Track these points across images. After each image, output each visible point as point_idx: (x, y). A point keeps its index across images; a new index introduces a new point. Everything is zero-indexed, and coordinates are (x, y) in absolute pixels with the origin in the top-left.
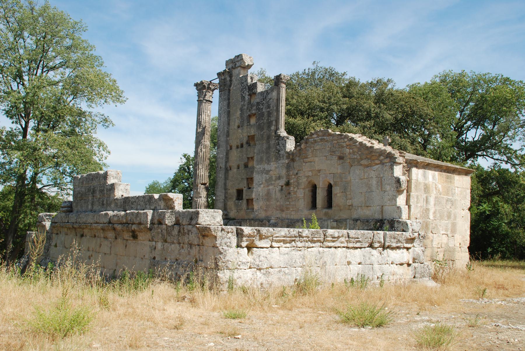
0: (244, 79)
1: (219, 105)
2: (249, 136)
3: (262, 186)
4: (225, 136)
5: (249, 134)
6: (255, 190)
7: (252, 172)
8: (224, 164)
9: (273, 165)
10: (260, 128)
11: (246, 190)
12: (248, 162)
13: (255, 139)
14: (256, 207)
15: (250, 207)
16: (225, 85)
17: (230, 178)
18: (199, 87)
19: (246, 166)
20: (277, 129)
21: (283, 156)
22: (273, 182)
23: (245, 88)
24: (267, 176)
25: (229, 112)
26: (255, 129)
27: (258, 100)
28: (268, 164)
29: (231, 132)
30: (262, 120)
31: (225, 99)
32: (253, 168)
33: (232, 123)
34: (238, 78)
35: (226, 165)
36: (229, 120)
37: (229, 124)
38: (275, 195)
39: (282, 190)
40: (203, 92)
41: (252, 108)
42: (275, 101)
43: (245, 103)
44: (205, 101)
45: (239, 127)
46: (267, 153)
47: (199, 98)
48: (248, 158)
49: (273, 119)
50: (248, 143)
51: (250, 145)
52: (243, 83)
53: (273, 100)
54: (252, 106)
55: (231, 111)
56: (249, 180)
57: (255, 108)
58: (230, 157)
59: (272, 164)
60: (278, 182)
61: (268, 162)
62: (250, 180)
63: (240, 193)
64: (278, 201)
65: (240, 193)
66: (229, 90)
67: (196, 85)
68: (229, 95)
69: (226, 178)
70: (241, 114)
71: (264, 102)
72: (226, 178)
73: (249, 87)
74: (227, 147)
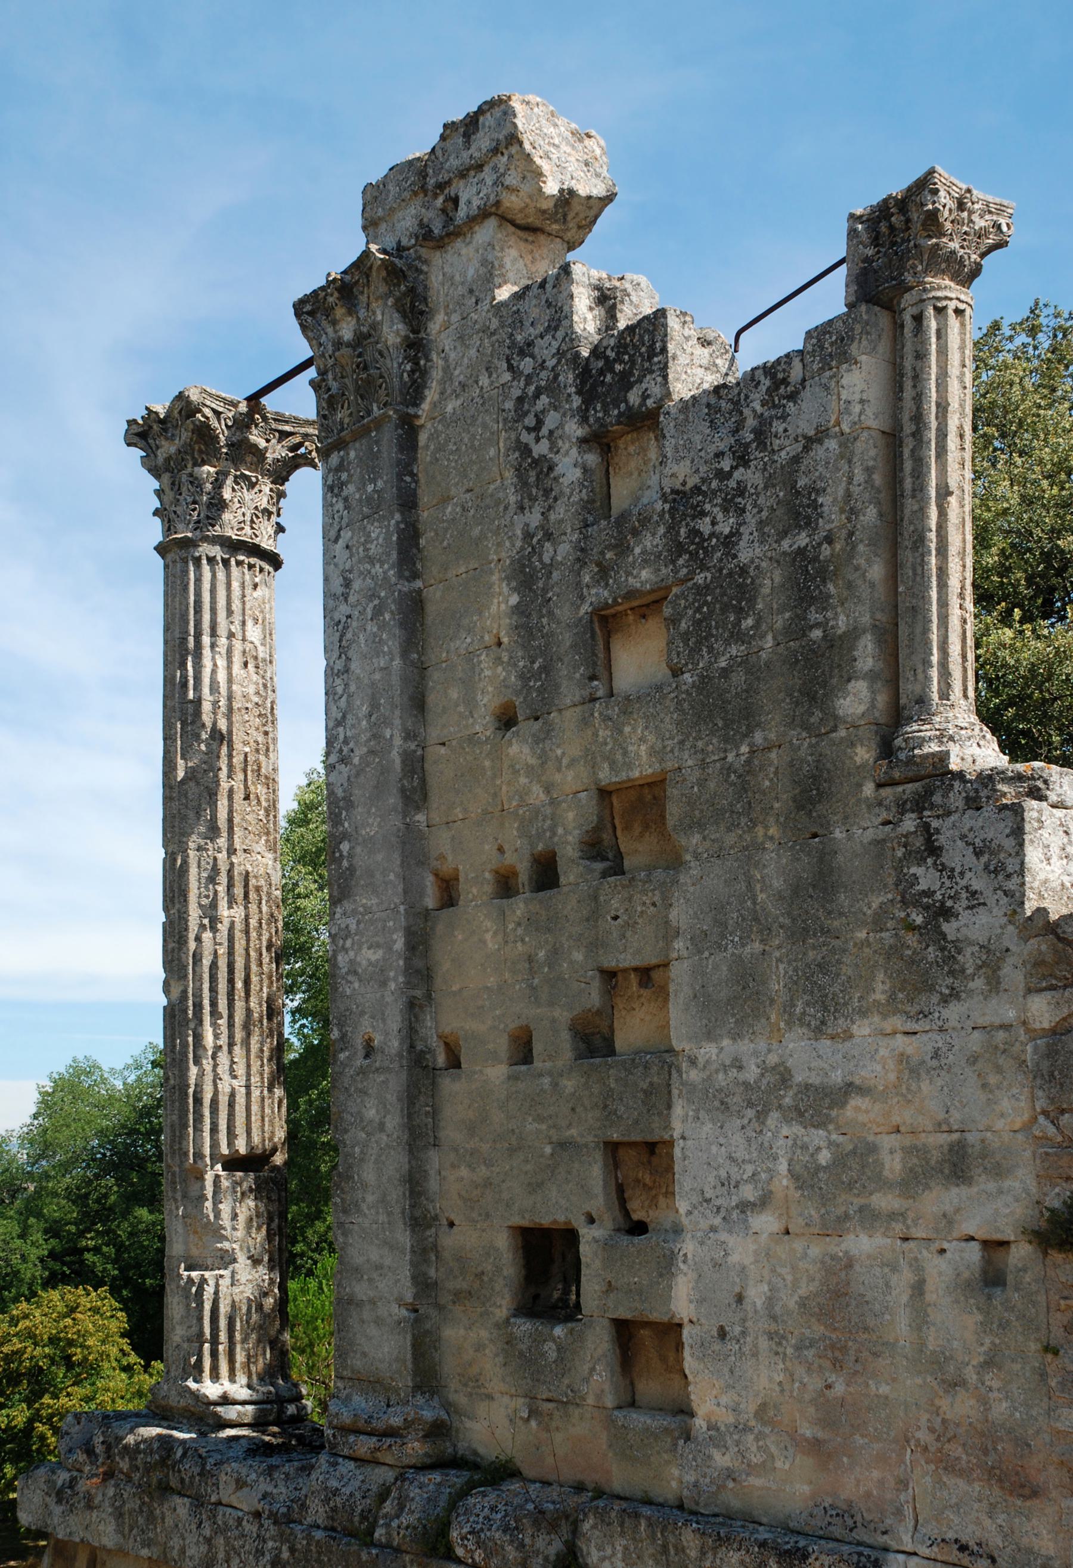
0: (533, 309)
1: (329, 559)
2: (604, 794)
3: (766, 1223)
4: (393, 800)
5: (605, 776)
6: (688, 1246)
7: (658, 1099)
8: (395, 1022)
9: (874, 1046)
10: (715, 708)
11: (607, 1245)
12: (607, 1012)
13: (674, 812)
14: (710, 1400)
15: (649, 1388)
16: (366, 390)
17: (451, 1133)
18: (168, 448)
19: (593, 1041)
20: (902, 709)
21: (992, 961)
22: (884, 1201)
23: (553, 388)
24: (817, 1137)
25: (413, 609)
26: (668, 724)
27: (682, 472)
28: (819, 1031)
30: (738, 636)
31: (374, 506)
32: (664, 1057)
33: (444, 695)
34: (481, 314)
35: (411, 1032)
36: (422, 670)
38: (921, 1319)
39: (992, 1277)
40: (196, 482)
41: (622, 549)
42: (869, 450)
43: (560, 512)
44: (216, 551)
45: (507, 721)
46: (800, 933)
48: (609, 976)
49: (852, 613)
50: (602, 850)
51: (617, 869)
52: (526, 349)
53: (847, 442)
54: (627, 528)
55: (434, 595)
56: (628, 1156)
57: (652, 541)
58: (444, 965)
59: (862, 1029)
60: (940, 1199)
61: (823, 1006)
62: (640, 1164)
63: (547, 1262)
64: (954, 1384)
65: (547, 1262)
66: (409, 429)
67: (144, 433)
69: (420, 1134)
70: (517, 610)
71: (750, 476)
73: (584, 372)
74: (411, 891)
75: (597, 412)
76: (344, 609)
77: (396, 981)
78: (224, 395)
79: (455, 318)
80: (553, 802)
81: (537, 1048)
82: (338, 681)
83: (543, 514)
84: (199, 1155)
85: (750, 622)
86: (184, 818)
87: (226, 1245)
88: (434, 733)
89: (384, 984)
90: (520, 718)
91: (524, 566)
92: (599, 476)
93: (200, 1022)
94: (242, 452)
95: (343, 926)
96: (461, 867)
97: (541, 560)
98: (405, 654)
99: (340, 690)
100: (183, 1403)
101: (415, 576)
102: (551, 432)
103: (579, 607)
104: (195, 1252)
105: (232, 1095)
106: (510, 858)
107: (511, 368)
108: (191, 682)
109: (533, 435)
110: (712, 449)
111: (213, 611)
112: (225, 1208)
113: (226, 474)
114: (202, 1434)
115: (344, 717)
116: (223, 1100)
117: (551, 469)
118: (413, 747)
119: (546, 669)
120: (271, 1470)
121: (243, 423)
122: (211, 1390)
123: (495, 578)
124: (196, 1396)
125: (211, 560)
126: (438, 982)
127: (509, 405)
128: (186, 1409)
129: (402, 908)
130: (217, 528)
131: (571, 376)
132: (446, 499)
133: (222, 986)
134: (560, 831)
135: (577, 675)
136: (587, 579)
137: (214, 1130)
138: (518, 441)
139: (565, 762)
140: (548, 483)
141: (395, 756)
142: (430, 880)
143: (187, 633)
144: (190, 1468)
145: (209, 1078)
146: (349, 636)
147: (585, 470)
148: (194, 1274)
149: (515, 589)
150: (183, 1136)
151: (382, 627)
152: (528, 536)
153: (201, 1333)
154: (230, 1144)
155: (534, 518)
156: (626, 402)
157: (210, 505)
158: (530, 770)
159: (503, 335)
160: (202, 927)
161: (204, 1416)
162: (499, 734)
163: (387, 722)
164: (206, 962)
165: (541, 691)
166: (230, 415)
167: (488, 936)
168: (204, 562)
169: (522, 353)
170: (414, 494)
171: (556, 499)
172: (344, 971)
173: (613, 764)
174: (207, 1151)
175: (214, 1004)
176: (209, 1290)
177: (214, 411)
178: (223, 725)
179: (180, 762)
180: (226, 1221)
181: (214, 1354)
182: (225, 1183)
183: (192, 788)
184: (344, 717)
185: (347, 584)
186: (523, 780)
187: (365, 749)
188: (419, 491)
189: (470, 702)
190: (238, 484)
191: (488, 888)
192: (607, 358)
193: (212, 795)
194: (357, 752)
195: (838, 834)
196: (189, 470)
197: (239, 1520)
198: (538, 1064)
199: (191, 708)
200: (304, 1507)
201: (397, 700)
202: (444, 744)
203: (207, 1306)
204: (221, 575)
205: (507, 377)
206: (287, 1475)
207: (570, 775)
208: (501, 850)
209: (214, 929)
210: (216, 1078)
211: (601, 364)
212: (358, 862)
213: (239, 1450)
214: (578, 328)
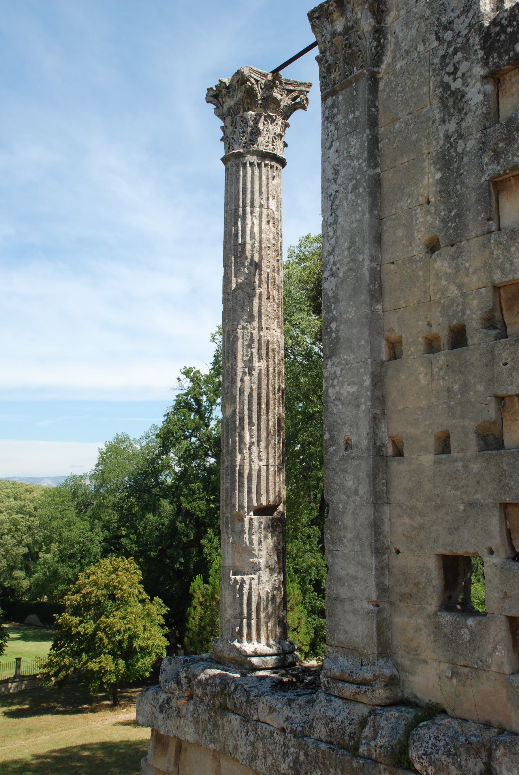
2: (496, 288)
4: (364, 297)
5: (498, 277)
17: (397, 496)
23: (465, 48)
29: (392, 276)
33: (394, 233)
35: (374, 434)
37: (378, 240)
43: (469, 121)
44: (254, 159)
45: (433, 247)
47: (229, 147)
48: (500, 399)
52: (448, 26)
58: (393, 394)
66: (374, 79)
68: (372, 103)
70: (440, 181)
72: (379, 497)
74: (374, 350)
75: (494, 59)
76: (334, 187)
77: (365, 404)
78: (260, 71)
79: (403, 12)
80: (463, 295)
81: (454, 444)
82: (330, 229)
83: (457, 123)
84: (241, 507)
86: (235, 311)
87: (255, 560)
88: (387, 257)
89: (358, 406)
90: (442, 246)
91: (445, 155)
92: (493, 98)
93: (243, 428)
94: (269, 102)
95: (332, 372)
96: (403, 336)
97: (456, 151)
98: (371, 211)
99: (331, 234)
100: (232, 655)
101: (376, 165)
102: (463, 74)
103: (481, 178)
104: (238, 564)
105: (259, 471)
106: (435, 329)
107: (438, 38)
108: (240, 233)
109: (452, 77)
111: (252, 193)
112: (255, 538)
113: (260, 115)
114: (243, 675)
115: (333, 249)
116: (255, 474)
117: (463, 96)
118: (375, 266)
119: (459, 216)
120: (290, 702)
121: (270, 86)
122: (248, 647)
123: (426, 164)
124: (240, 652)
125: (251, 164)
126: (389, 404)
127: (436, 61)
128: (233, 659)
129: (369, 361)
130: (255, 146)
131: (477, 39)
132: (395, 120)
133: (255, 407)
134: (468, 312)
135: (480, 218)
136: (486, 160)
137: (250, 491)
138: (442, 81)
139: (471, 270)
140: (461, 105)
141: (365, 271)
142: (384, 343)
143: (238, 206)
144: (239, 697)
145: (247, 461)
146: (337, 202)
147: (485, 95)
148: (238, 577)
149: (439, 169)
150: (232, 496)
151: (357, 197)
152: (447, 137)
153: (242, 613)
154: (258, 500)
155: (452, 127)
156: (514, 50)
157: (252, 133)
158: (448, 276)
159: (433, 19)
160: (244, 373)
161: (243, 663)
162: (428, 255)
163: (360, 251)
164: (246, 394)
165: (455, 229)
166: (263, 82)
167: (421, 377)
168: (248, 165)
169: (445, 29)
170: (376, 118)
171: (466, 114)
172: (332, 398)
173: (503, 271)
174: (246, 504)
175: (250, 418)
176: (246, 587)
177: (255, 80)
178: (256, 259)
179: (234, 279)
180: (256, 546)
181: (249, 625)
182: (256, 523)
183: (240, 294)
184: (333, 249)
185: (336, 172)
186: (444, 282)
187: (346, 268)
188: (379, 116)
189: (410, 238)
190: (266, 120)
191: (422, 348)
192: (502, 25)
193: (251, 297)
194: (342, 270)
196: (241, 114)
197: (272, 733)
198: (454, 454)
199: (240, 248)
200: (311, 727)
201: (367, 238)
202: (393, 263)
203: (245, 597)
204: (257, 173)
205: (436, 44)
206: (300, 705)
207: (474, 278)
208: (429, 325)
209: (251, 374)
210: (251, 461)
211: (497, 29)
212: (342, 334)
213: (266, 686)
214: (482, 9)
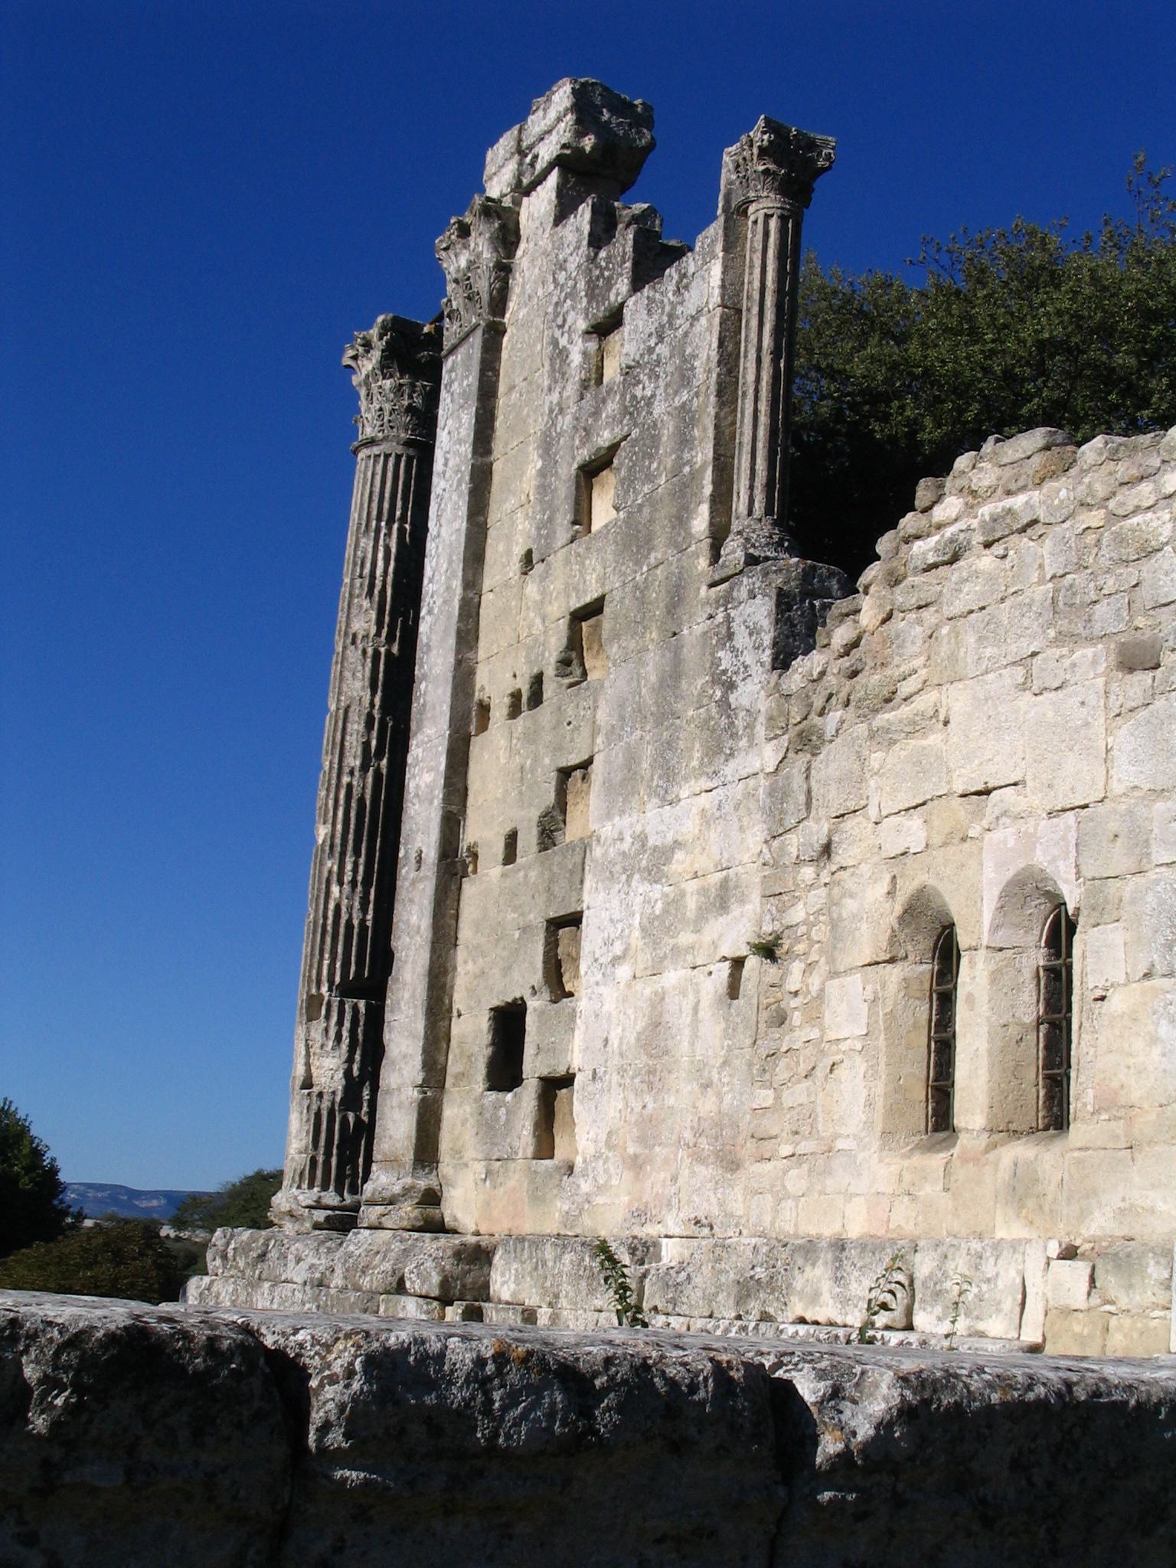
22: (685, 938)
38: (695, 1036)
71: (663, 350)
85: (655, 465)
110: (647, 331)
119: (551, 519)
127: (550, 309)
136: (577, 442)
195: (685, 632)
